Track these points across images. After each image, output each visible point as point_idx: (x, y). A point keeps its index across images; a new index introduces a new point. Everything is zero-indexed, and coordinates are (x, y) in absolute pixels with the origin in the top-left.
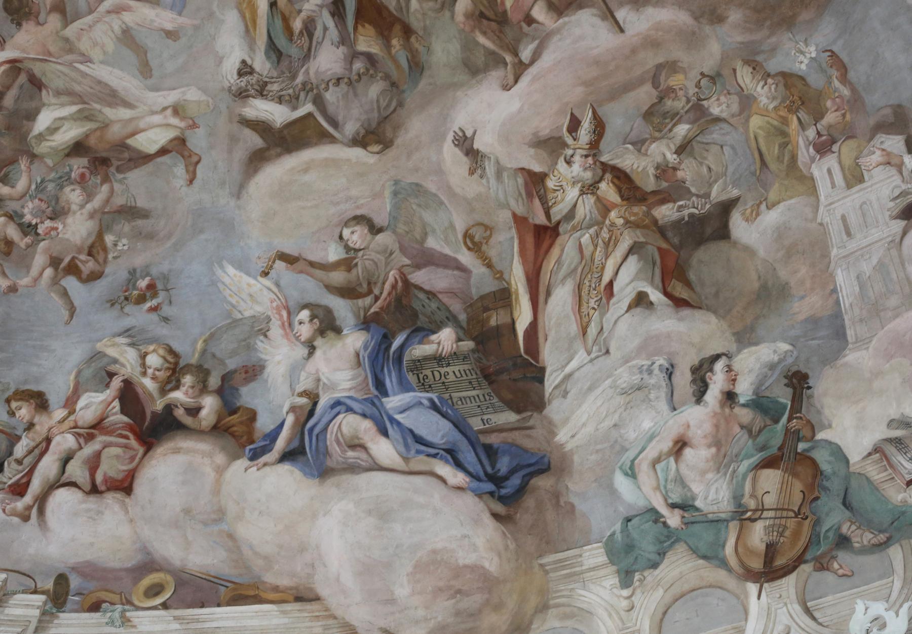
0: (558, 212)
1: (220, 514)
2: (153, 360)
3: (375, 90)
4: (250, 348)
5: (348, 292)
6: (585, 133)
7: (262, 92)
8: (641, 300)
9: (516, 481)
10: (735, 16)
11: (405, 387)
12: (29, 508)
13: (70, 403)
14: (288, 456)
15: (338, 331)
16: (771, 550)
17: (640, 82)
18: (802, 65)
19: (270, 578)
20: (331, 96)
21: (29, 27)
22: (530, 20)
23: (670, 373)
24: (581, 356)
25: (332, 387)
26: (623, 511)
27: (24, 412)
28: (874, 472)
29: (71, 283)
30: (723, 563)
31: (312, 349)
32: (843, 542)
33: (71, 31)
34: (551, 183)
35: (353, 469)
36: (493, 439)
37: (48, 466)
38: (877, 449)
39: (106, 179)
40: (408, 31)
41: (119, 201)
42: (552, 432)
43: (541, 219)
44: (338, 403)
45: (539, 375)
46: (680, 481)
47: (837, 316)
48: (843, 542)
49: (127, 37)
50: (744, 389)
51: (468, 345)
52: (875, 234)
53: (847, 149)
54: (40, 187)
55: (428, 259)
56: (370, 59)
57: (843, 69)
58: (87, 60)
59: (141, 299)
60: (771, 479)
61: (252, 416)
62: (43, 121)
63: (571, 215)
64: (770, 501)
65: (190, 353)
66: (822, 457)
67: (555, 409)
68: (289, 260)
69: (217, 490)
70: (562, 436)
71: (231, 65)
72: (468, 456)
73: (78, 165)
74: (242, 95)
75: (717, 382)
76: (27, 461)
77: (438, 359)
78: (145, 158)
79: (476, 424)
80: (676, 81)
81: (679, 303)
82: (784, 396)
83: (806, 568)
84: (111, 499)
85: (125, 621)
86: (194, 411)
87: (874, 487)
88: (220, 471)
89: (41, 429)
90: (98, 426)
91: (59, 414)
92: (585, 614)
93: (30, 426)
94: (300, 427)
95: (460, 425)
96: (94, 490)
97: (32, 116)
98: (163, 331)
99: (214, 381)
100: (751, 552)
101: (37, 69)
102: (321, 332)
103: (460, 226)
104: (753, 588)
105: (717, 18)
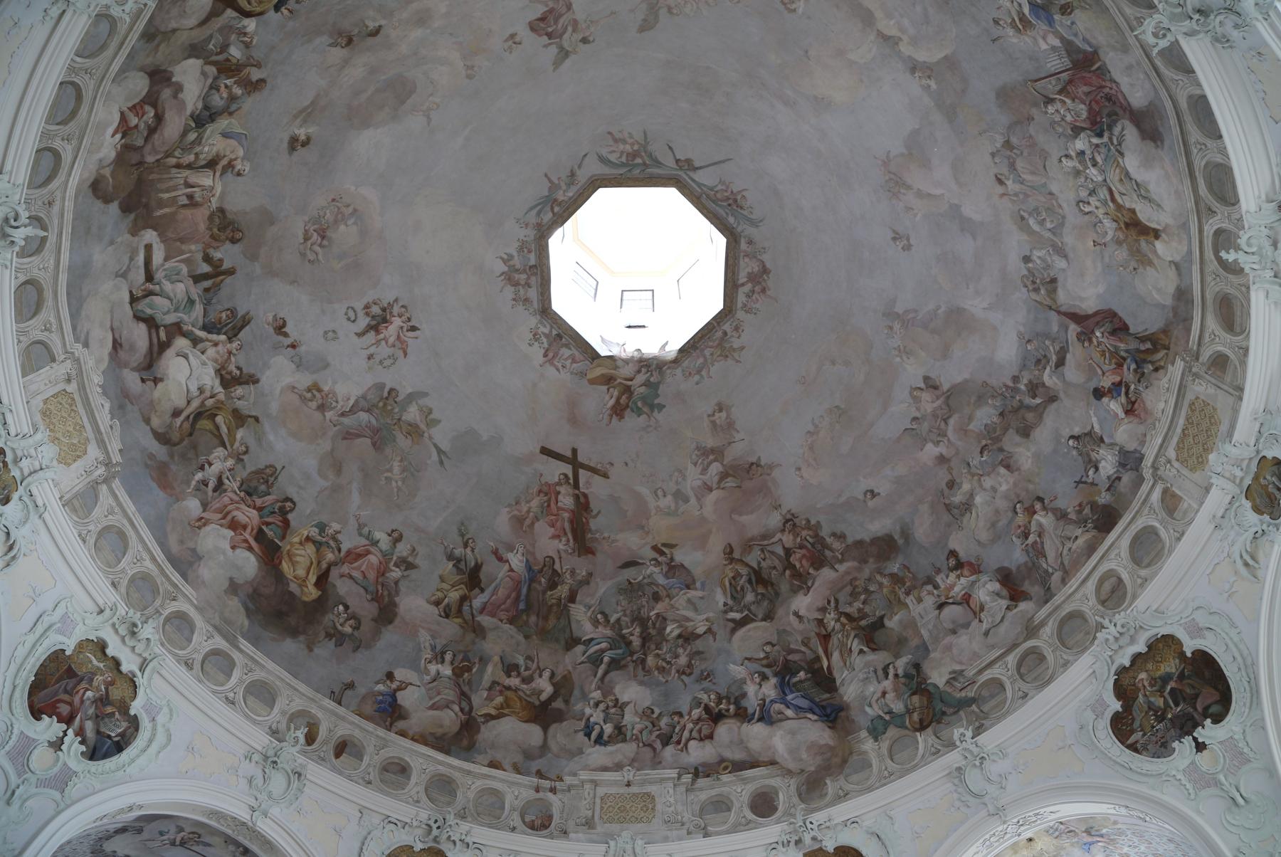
0: (830, 629)
1: (742, 742)
2: (712, 697)
3: (766, 603)
4: (741, 688)
5: (768, 666)
6: (833, 604)
7: (731, 610)
8: (861, 651)
9: (833, 715)
10: (871, 560)
11: (792, 692)
13: (689, 714)
14: (760, 720)
15: (768, 678)
16: (921, 721)
17: (845, 586)
18: (895, 570)
19: (761, 759)
20: (753, 608)
22: (809, 574)
23: (875, 672)
24: (846, 672)
25: (769, 696)
26: (870, 718)
27: (676, 719)
28: (949, 690)
29: (684, 677)
30: (907, 728)
31: (761, 686)
32: (944, 713)
33: (672, 602)
34: (825, 621)
35: (781, 720)
36: (824, 703)
37: (686, 734)
38: (947, 682)
40: (772, 584)
41: (694, 650)
42: (841, 697)
43: (824, 633)
44: (772, 701)
45: (834, 680)
46: (887, 705)
47: (924, 643)
48: (944, 713)
49: (689, 601)
50: (900, 672)
51: (809, 675)
52: (930, 616)
53: (915, 592)
54: (670, 650)
55: (791, 651)
56: (763, 595)
57: (908, 569)
58: (678, 610)
59: (706, 679)
60: (916, 699)
61: (746, 709)
62: (668, 629)
63: (834, 629)
64: (917, 705)
65: (723, 692)
66: (930, 688)
67: (841, 690)
68: (749, 659)
69: (739, 734)
70: (845, 698)
71: (721, 604)
72: (817, 710)
73: (680, 641)
74: (726, 612)
75: (891, 672)
77: (801, 681)
78: (700, 636)
79: (817, 699)
80: (857, 583)
81: (874, 650)
82: (914, 672)
83: (934, 724)
84: (707, 742)
85: (718, 779)
86: (728, 710)
87: (949, 694)
88: (739, 728)
89: (682, 723)
90: (699, 719)
91: (687, 717)
92: (865, 753)
93: (679, 722)
94: (761, 710)
95: (812, 701)
96: (701, 740)
97: (665, 629)
98: (714, 687)
99: (732, 700)
100: (915, 722)
102: (763, 680)
103: (800, 639)
104: (918, 734)
105: (866, 562)
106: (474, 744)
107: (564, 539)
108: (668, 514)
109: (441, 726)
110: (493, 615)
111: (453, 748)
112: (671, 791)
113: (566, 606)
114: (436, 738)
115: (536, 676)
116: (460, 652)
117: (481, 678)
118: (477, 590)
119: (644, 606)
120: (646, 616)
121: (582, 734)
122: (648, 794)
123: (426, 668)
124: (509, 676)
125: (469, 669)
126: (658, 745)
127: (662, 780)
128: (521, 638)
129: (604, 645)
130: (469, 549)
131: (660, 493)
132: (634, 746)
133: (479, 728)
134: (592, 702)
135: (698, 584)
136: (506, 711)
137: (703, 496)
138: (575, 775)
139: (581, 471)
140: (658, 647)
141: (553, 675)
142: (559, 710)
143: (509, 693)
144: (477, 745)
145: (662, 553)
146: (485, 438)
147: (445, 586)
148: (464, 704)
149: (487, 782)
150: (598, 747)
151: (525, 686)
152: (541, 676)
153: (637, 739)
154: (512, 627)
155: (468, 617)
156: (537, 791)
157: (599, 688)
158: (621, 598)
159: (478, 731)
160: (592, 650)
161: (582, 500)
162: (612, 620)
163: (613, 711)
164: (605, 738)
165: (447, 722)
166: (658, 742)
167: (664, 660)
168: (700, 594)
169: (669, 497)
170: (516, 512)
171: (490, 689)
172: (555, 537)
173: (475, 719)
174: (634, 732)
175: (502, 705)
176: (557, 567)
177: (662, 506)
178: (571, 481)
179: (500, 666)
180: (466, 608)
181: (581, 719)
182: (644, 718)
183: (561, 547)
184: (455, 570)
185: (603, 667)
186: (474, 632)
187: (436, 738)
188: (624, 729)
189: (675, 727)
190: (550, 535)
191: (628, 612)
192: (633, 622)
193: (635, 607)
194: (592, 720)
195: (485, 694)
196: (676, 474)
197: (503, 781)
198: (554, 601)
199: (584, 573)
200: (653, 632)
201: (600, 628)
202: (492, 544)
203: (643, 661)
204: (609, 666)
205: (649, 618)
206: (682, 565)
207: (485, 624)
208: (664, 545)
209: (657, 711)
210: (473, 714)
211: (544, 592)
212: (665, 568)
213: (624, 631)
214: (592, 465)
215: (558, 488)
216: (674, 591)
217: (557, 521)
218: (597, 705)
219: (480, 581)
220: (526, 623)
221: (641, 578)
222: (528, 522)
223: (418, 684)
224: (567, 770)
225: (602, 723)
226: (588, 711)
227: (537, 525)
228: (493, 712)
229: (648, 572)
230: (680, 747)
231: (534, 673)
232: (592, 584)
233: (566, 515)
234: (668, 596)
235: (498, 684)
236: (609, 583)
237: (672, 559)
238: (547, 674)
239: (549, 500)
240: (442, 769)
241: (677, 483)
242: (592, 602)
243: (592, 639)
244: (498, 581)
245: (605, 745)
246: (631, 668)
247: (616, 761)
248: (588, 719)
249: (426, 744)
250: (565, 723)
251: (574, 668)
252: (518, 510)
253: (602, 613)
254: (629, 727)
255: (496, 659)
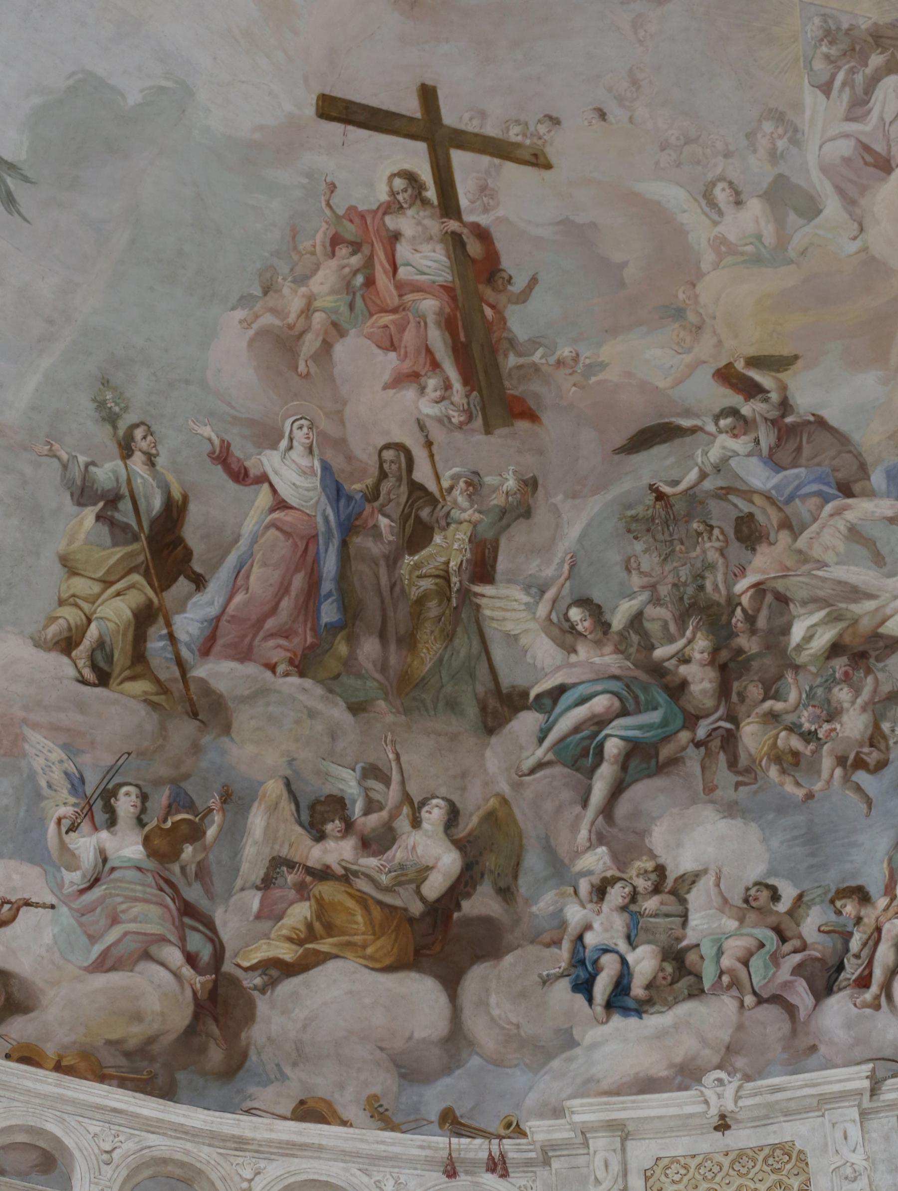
12: (877, 997)
21: (763, 549)
27: (850, 908)
29: (861, 777)
33: (801, 542)
39: (869, 671)
41: (886, 688)
49: (854, 534)
54: (811, 695)
58: (823, 565)
62: (798, 632)
73: (840, 664)
76: (864, 954)
91: (882, 902)
93: (859, 920)
97: (786, 630)
101: (780, 586)
106: (245, 1056)
107: (432, 383)
108: (757, 260)
109: (137, 1017)
110: (244, 655)
111: (182, 1077)
112: (854, 1132)
113: (465, 594)
114: (128, 1055)
115: (403, 823)
116: (158, 783)
117: (236, 854)
118: (183, 584)
119: (711, 567)
120: (720, 597)
121: (564, 985)
122: (785, 1149)
123: (62, 844)
124: (320, 837)
125: (195, 833)
126: (801, 996)
127: (824, 1102)
128: (338, 713)
129: (601, 704)
130: (138, 457)
131: (721, 194)
132: (728, 1004)
133: (251, 1006)
134: (584, 887)
135: (877, 479)
136: (325, 946)
137: (863, 190)
138: (558, 1112)
139: (459, 158)
140: (772, 691)
141: (453, 815)
142: (487, 921)
143: (327, 890)
144: (253, 1057)
145: (752, 390)
146: (134, 98)
147: (80, 586)
148: (197, 942)
149: (296, 1164)
150: (617, 1021)
151: (373, 862)
152: (416, 823)
153: (735, 983)
154: (308, 683)
155: (168, 672)
156: (451, 1172)
157: (601, 839)
158: (639, 546)
159: (250, 1017)
160: (565, 724)
161: (474, 248)
162: (618, 620)
163: (651, 904)
164: (638, 990)
165: (152, 1003)
166: (801, 985)
167: (793, 728)
168: (884, 507)
169: (755, 207)
170: (268, 319)
171: (267, 883)
172: (399, 380)
173: (234, 981)
174: (726, 962)
175: (310, 927)
176: (423, 474)
177: (732, 238)
178: (431, 194)
179: (287, 807)
180: (156, 645)
181: (556, 943)
182: (752, 916)
183: (428, 408)
184: (105, 530)
185: (605, 774)
186: (195, 715)
187: (128, 1055)
188: (691, 958)
189: (847, 936)
190: (387, 376)
191: (664, 590)
192: (682, 620)
193: (684, 573)
194: (590, 939)
195: (255, 901)
196: (768, 127)
197: (346, 1156)
198: (427, 584)
199: (511, 483)
200: (749, 644)
201: (584, 652)
202: (207, 431)
203: (730, 740)
204: (624, 767)
205: (732, 603)
206: (821, 423)
207: (221, 686)
208: (754, 362)
209: (788, 893)
210: (227, 967)
211: (393, 561)
212: (767, 437)
213: (659, 653)
214: (491, 130)
215: (391, 222)
216: (802, 508)
217: (402, 329)
218: (600, 891)
219: (188, 554)
220: (349, 664)
221: (693, 476)
222: (310, 344)
223: (50, 899)
224: (531, 1100)
225: (622, 946)
226: (575, 914)
227: (340, 349)
228: (287, 953)
229: (715, 454)
230: (868, 996)
231: (393, 816)
232: (541, 514)
233: (429, 305)
234: (786, 524)
235: (291, 865)
236: (595, 505)
237: (785, 406)
238: (434, 815)
239: (369, 263)
240: (161, 1145)
241: (774, 156)
242: (549, 572)
243: (562, 689)
244: (243, 544)
245: (639, 1009)
246: (693, 760)
247: (678, 1060)
248: (580, 938)
249: (102, 1078)
250: (509, 959)
251: (517, 786)
252: (274, 311)
253: (584, 602)
254: (708, 950)
255: (274, 788)
